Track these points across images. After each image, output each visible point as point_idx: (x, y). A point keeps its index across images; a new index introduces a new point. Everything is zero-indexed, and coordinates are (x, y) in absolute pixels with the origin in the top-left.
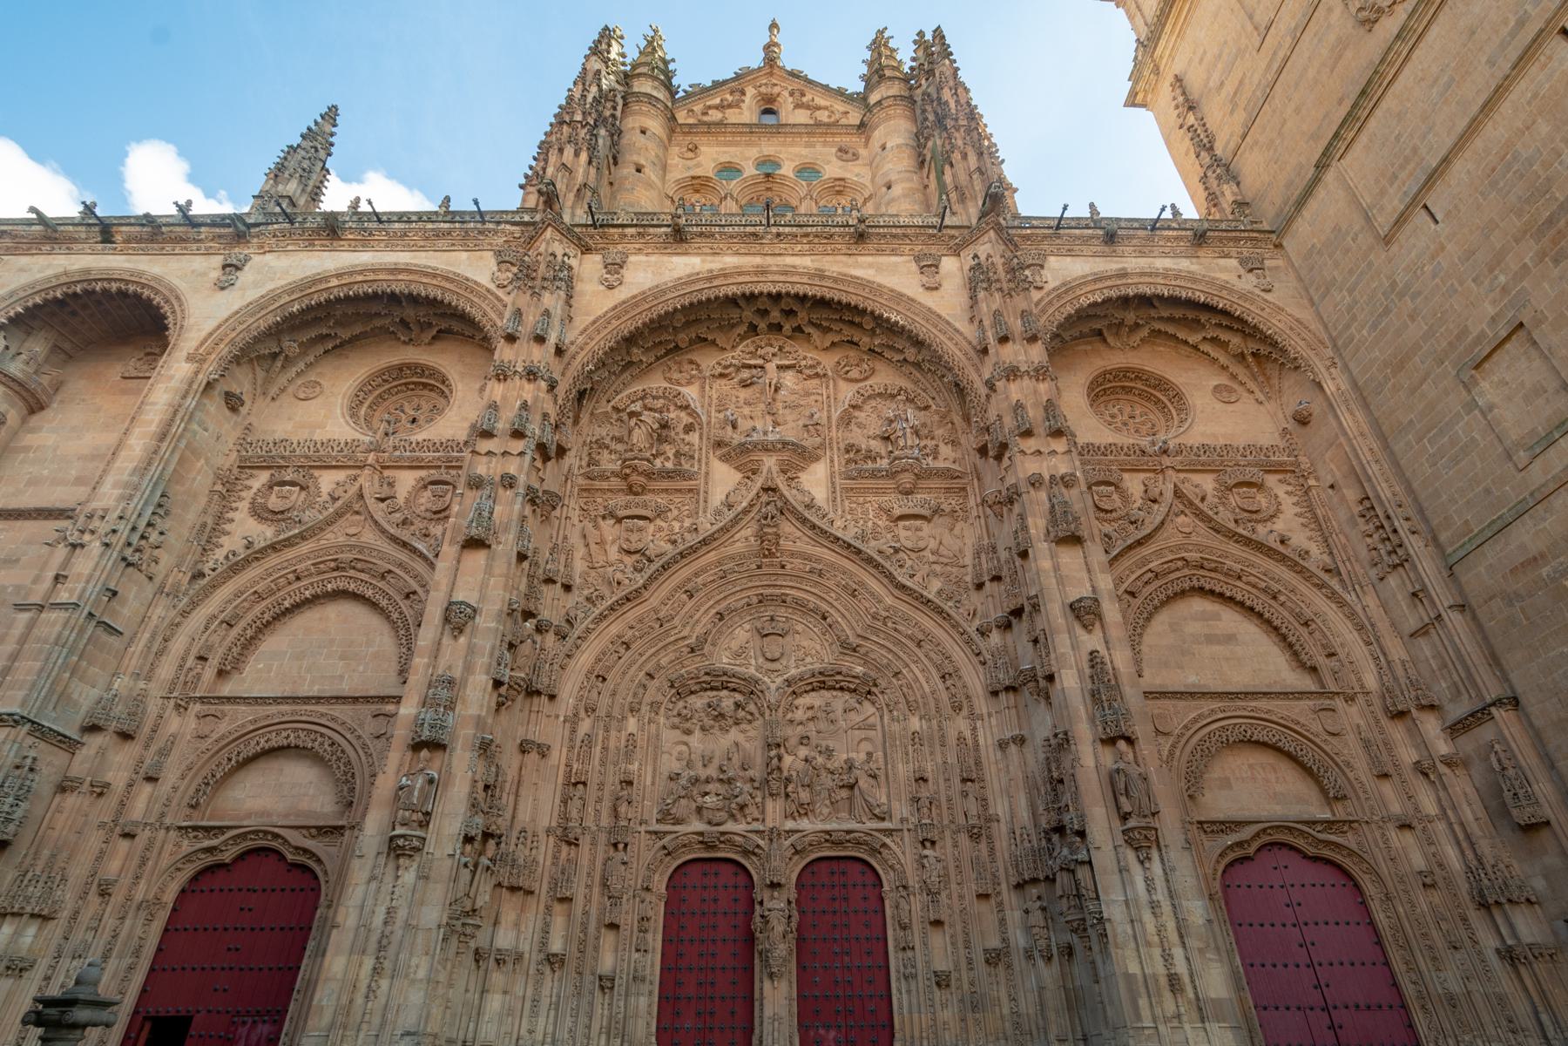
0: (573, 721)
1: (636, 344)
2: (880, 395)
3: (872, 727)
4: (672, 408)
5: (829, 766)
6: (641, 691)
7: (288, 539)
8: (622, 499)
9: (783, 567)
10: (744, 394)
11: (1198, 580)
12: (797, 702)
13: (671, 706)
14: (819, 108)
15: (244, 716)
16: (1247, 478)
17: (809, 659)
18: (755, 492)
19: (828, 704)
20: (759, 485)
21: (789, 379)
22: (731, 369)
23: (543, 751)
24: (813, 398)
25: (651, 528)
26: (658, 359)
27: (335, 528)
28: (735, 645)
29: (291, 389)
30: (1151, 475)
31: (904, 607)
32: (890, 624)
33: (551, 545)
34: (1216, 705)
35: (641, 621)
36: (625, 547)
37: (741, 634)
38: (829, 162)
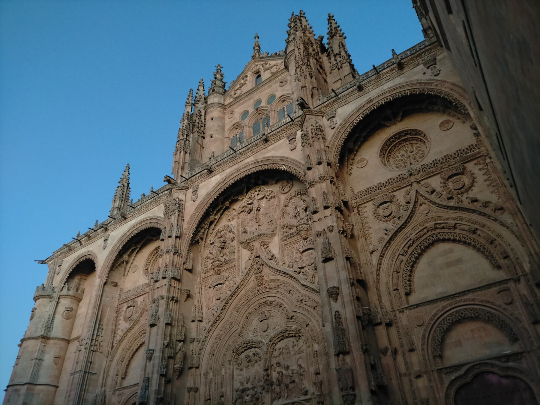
0: (206, 375)
1: (211, 215)
2: (294, 196)
3: (302, 352)
4: (227, 233)
5: (288, 374)
6: (224, 356)
7: (131, 327)
8: (216, 277)
9: (267, 288)
10: (250, 216)
11: (437, 236)
12: (276, 347)
13: (235, 360)
14: (272, 67)
15: (127, 392)
16: (455, 172)
17: (277, 327)
18: (252, 260)
19: (287, 345)
20: (253, 257)
21: (263, 203)
22: (244, 208)
23: (197, 390)
24: (271, 208)
25: (224, 286)
26: (221, 215)
27: (142, 318)
28: (252, 328)
29: (130, 270)
30: (409, 188)
31: (308, 293)
32: (304, 303)
33: (193, 306)
34: (444, 303)
35: (223, 327)
36: (216, 298)
37: (255, 322)
38: (277, 91)
